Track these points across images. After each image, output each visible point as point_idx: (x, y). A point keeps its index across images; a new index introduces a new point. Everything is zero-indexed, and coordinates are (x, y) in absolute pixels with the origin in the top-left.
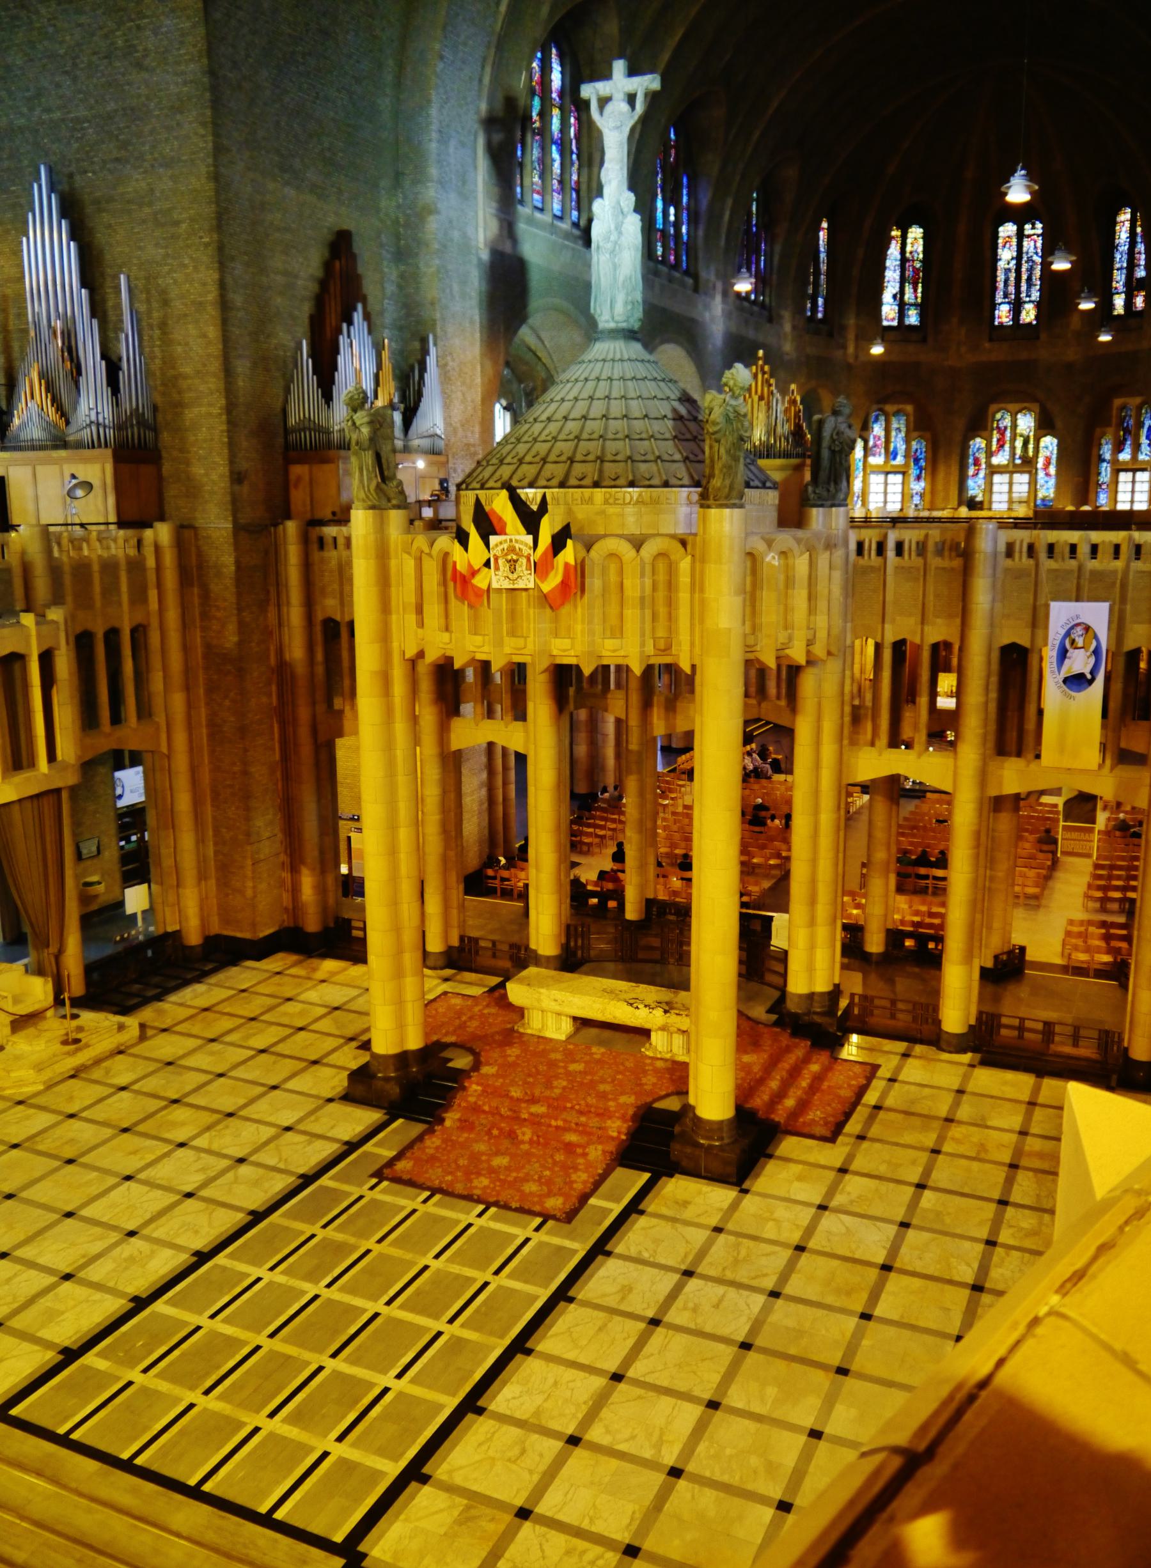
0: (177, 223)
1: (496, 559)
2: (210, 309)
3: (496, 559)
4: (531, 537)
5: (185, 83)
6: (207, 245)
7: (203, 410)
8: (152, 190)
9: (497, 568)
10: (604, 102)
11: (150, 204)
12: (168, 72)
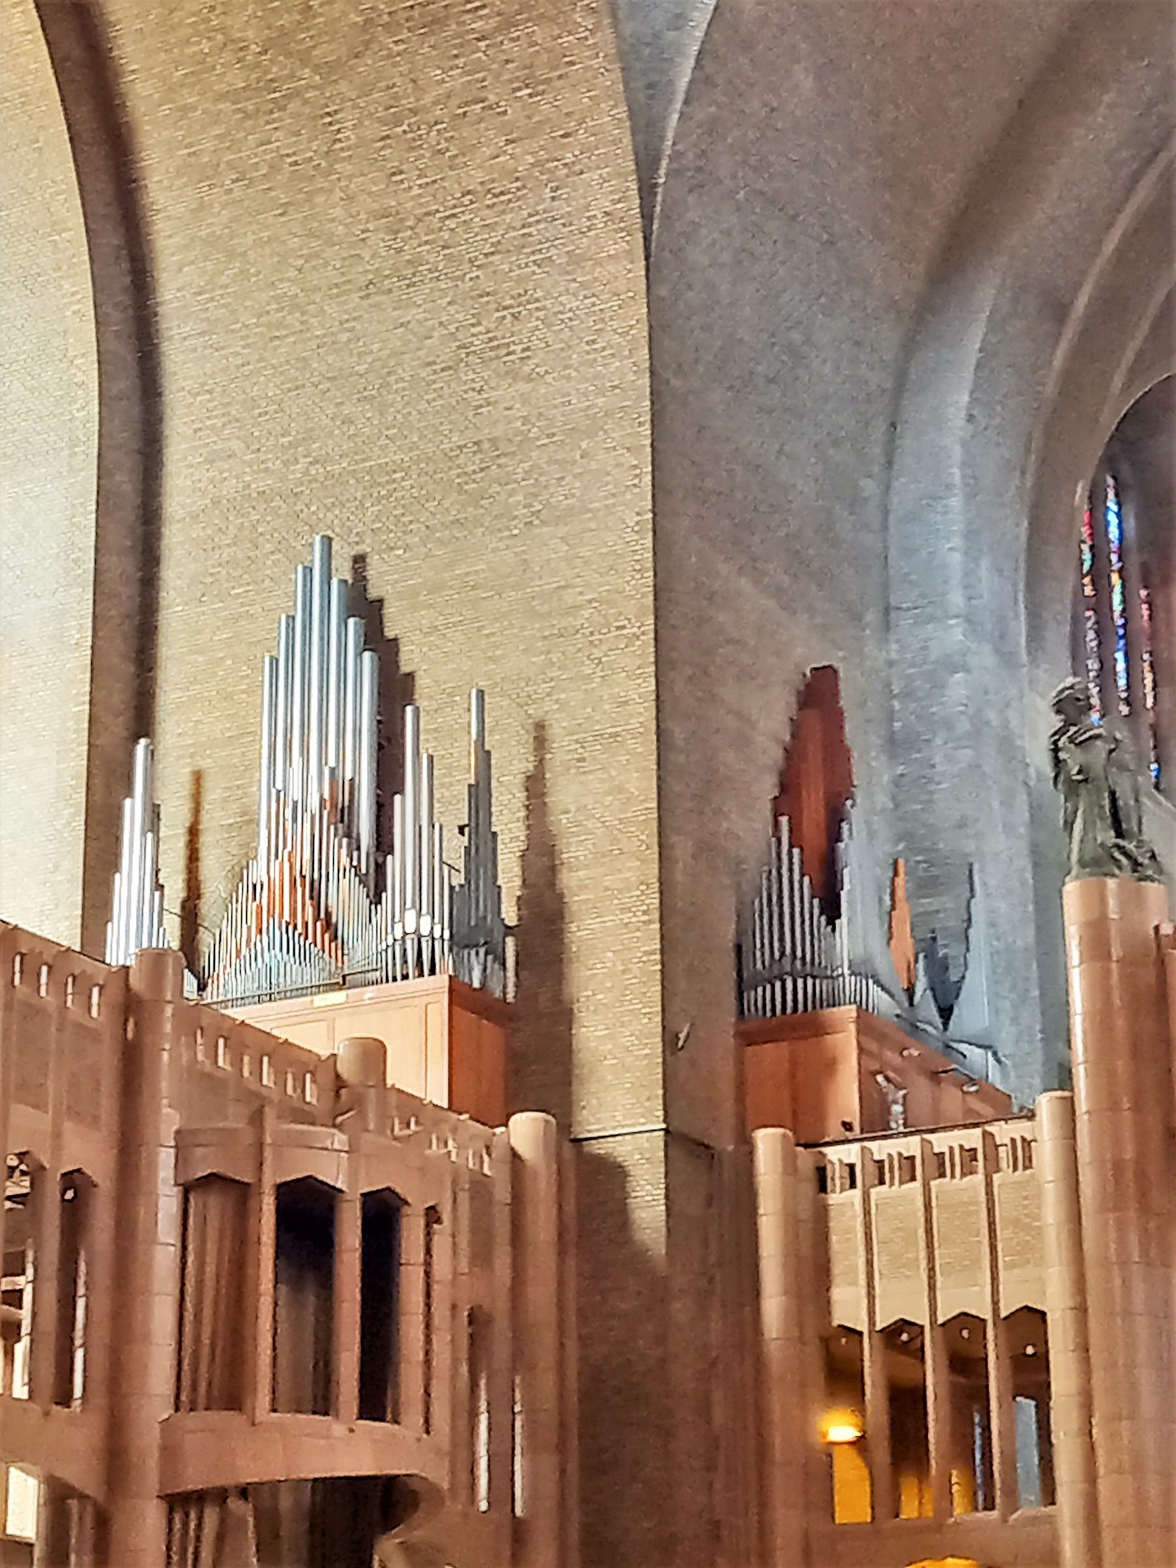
12: (568, 378)
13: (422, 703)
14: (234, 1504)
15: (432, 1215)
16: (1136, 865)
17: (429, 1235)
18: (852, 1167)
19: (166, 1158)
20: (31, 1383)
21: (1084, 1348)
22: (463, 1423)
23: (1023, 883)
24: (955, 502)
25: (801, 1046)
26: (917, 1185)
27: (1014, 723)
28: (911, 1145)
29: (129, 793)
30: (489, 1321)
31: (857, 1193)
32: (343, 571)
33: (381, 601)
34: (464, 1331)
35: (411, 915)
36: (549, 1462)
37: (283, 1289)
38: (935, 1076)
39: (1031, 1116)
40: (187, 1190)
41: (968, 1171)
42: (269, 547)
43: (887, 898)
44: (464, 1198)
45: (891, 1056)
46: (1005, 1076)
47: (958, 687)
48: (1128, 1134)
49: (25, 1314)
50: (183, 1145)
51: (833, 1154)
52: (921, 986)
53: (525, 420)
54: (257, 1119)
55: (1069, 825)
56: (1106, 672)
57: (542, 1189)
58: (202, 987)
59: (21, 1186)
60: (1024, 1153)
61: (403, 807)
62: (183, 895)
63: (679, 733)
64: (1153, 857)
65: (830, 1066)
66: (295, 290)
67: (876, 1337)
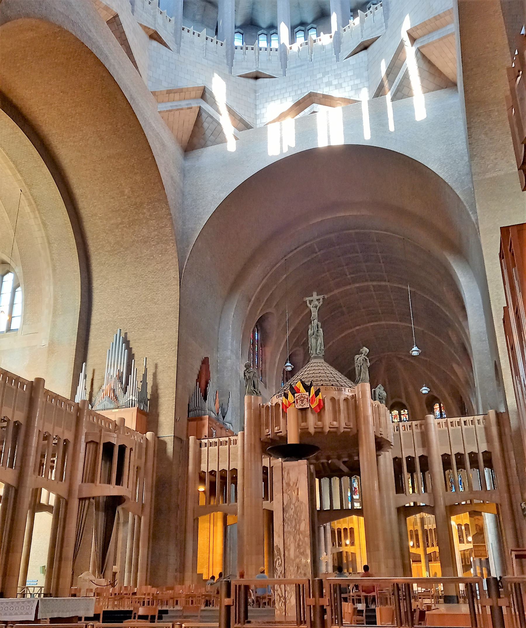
0: (164, 344)
1: (297, 400)
2: (172, 368)
3: (297, 400)
4: (308, 393)
5: (171, 307)
6: (173, 350)
7: (166, 399)
8: (156, 336)
9: (297, 403)
10: (311, 302)
11: (154, 340)
13: (136, 359)
14: (91, 500)
15: (131, 449)
16: (257, 393)
17: (130, 452)
18: (206, 443)
19: (83, 437)
20: (55, 477)
21: (243, 475)
22: (134, 487)
23: (238, 396)
24: (230, 331)
25: (199, 422)
26: (217, 447)
27: (238, 369)
28: (216, 440)
29: (82, 372)
30: (140, 468)
31: (207, 448)
32: (123, 335)
33: (129, 341)
34: (136, 470)
35: (131, 396)
36: (149, 494)
37: (103, 462)
38: (221, 428)
39: (237, 436)
40: (87, 443)
41: (226, 445)
42: (110, 330)
43: (215, 397)
44: (137, 446)
45: (214, 425)
46: (233, 428)
47: (229, 362)
48: (253, 439)
49: (55, 465)
50: (87, 435)
51: (203, 441)
52: (220, 412)
53: (157, 311)
54: (101, 431)
55: (246, 386)
56: (254, 361)
57: (151, 446)
58: (92, 407)
59: (56, 441)
60: (235, 442)
61: (131, 377)
62: (90, 391)
63: (180, 367)
64: (260, 392)
65: (203, 426)
66: (117, 286)
67: (208, 473)
